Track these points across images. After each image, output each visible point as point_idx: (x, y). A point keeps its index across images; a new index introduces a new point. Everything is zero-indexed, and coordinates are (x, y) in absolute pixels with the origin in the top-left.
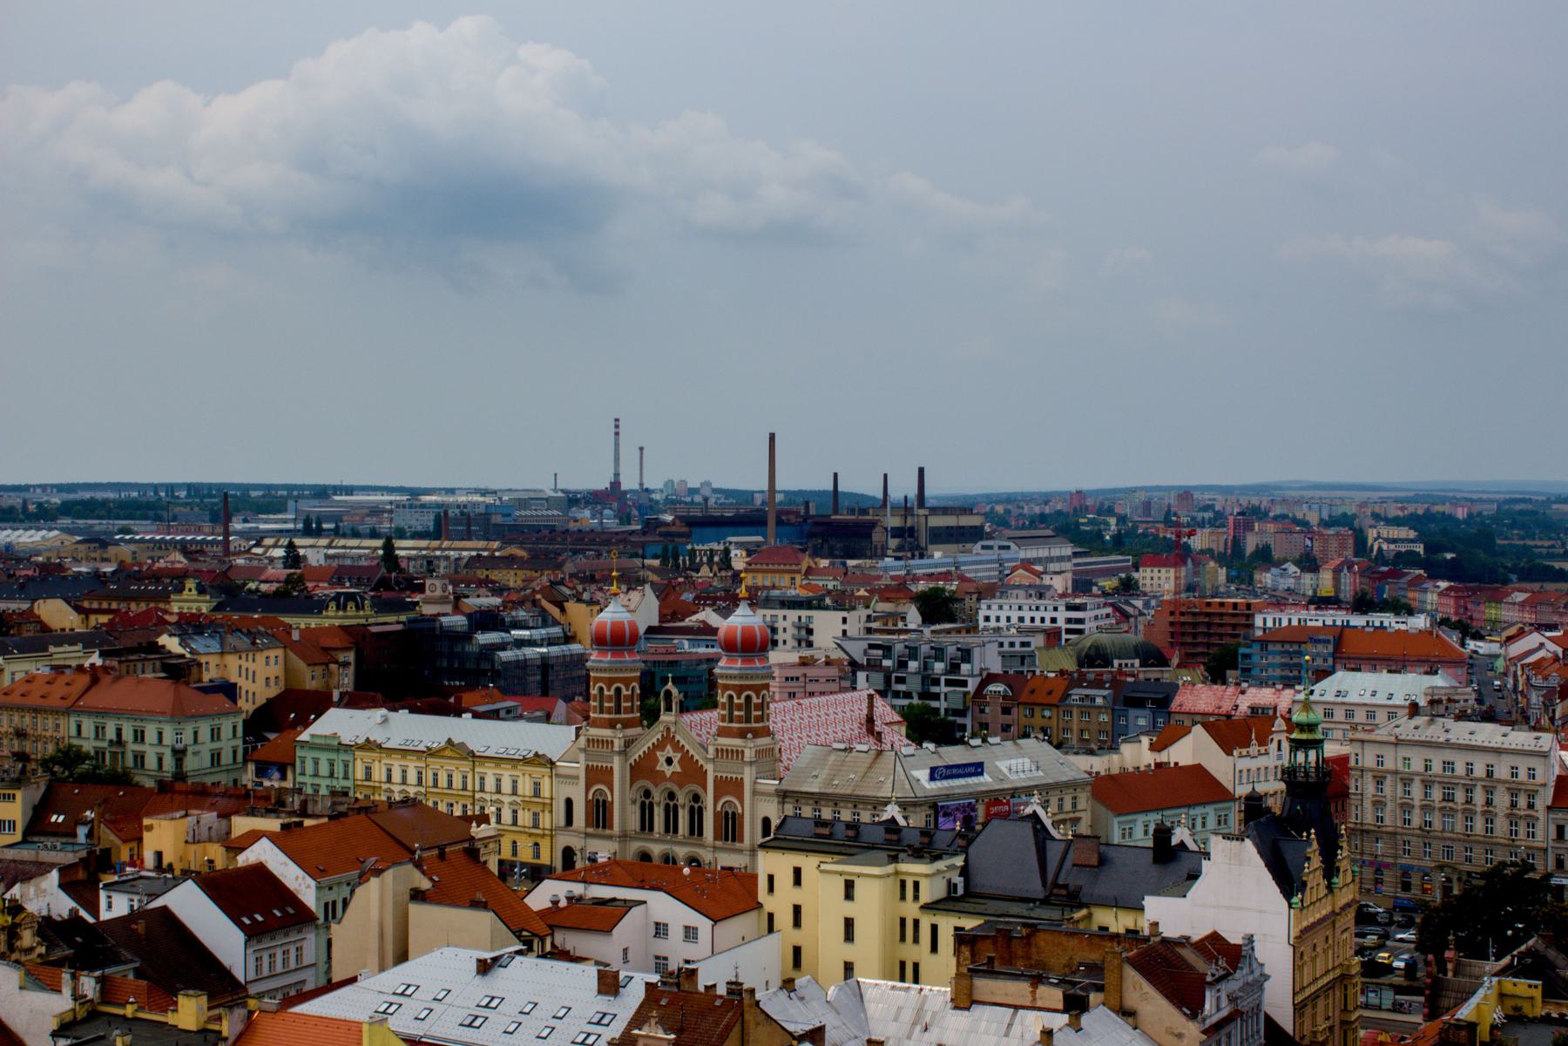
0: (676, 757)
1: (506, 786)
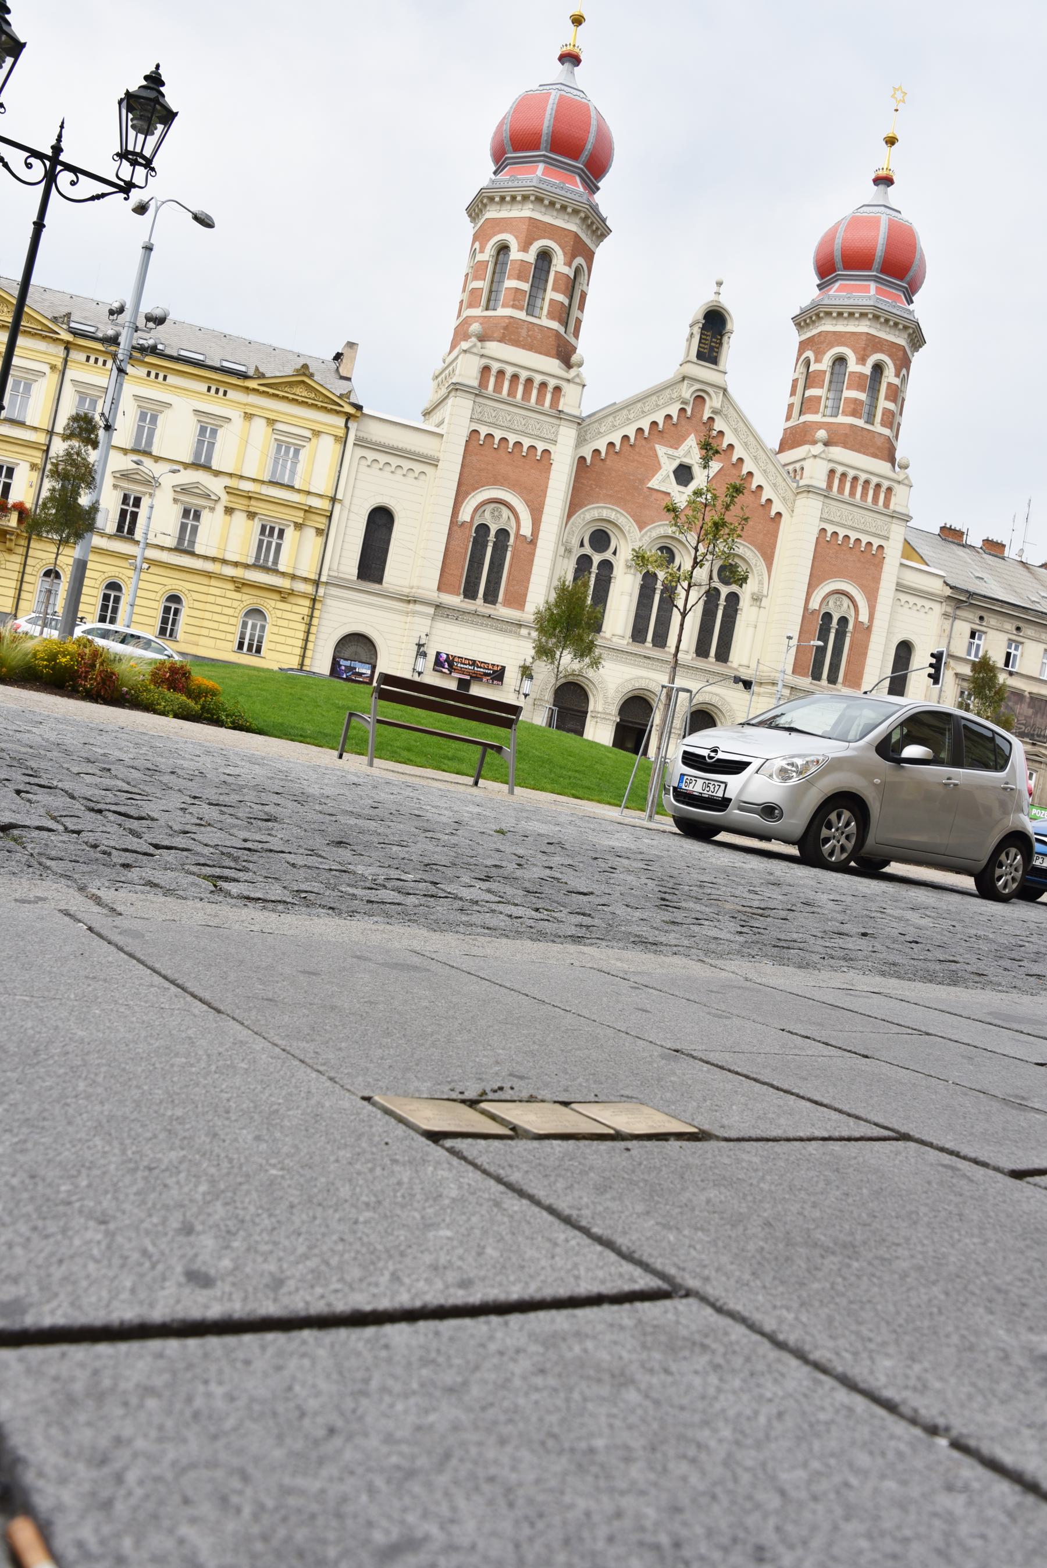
1: (175, 436)
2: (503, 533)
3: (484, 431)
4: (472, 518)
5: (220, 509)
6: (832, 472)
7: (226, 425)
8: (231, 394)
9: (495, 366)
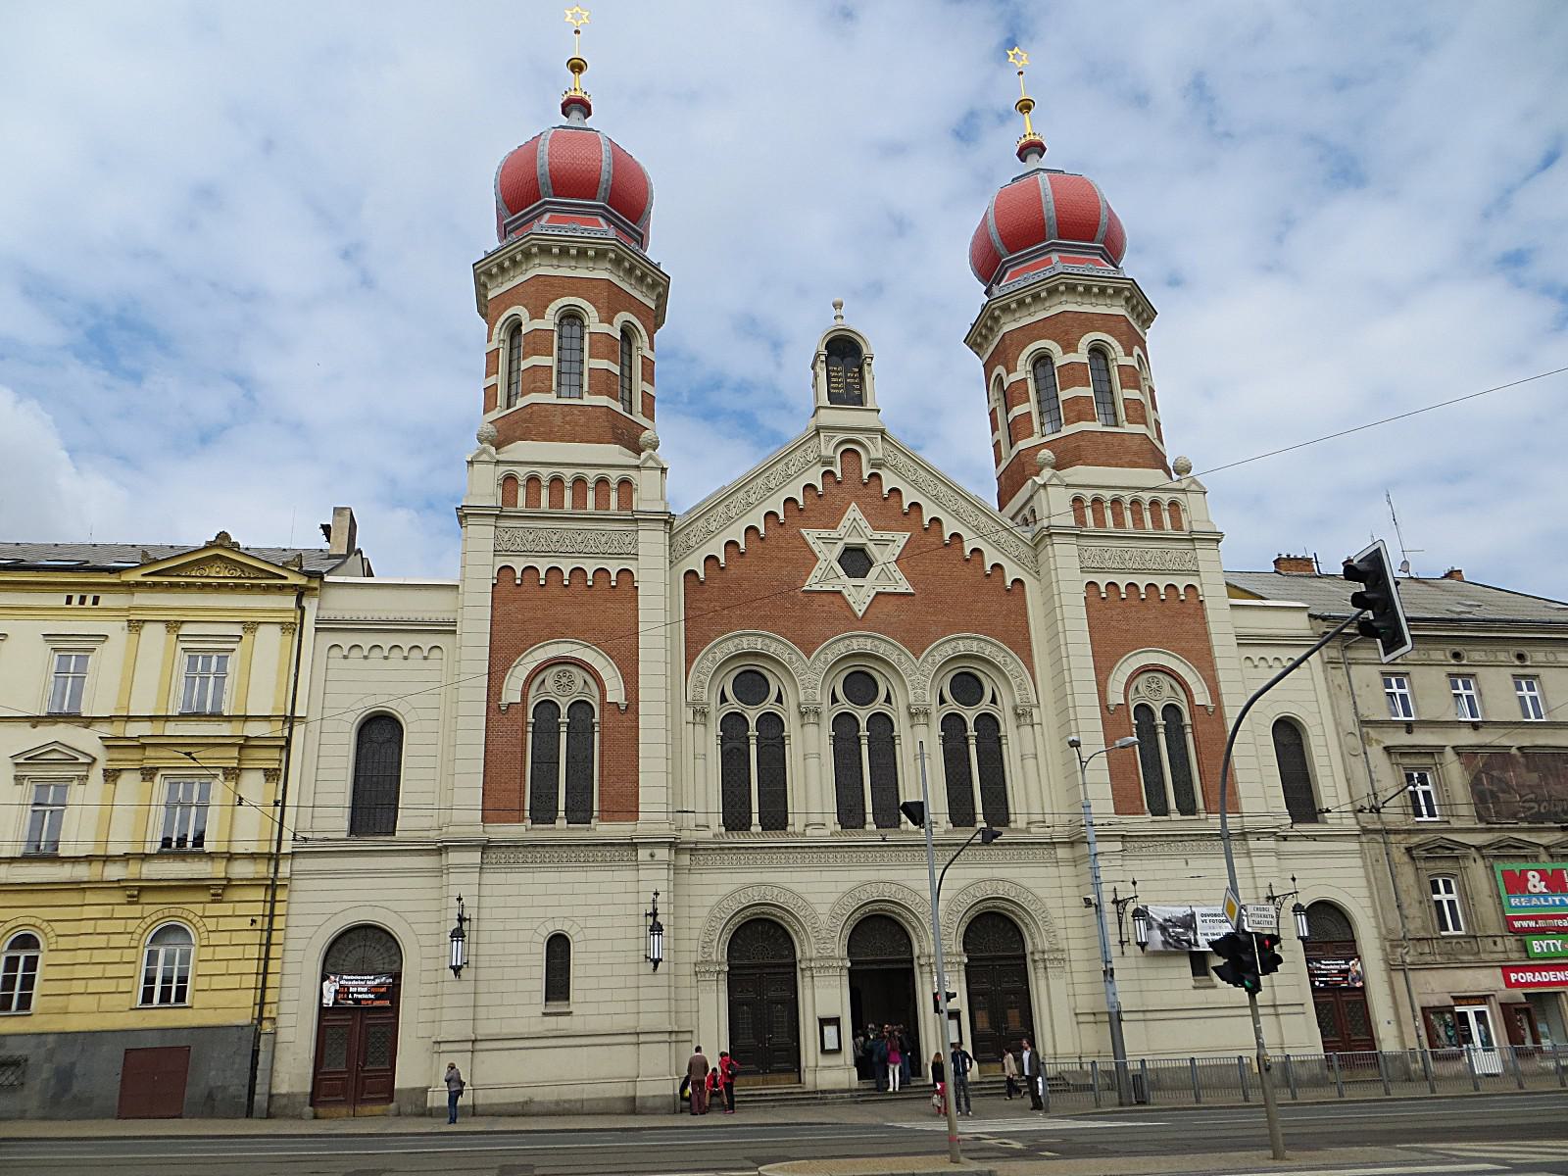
0: (888, 550)
2: (580, 707)
3: (519, 565)
4: (524, 695)
5: (97, 773)
6: (1077, 500)
7: (99, 647)
8: (105, 600)
9: (522, 473)
